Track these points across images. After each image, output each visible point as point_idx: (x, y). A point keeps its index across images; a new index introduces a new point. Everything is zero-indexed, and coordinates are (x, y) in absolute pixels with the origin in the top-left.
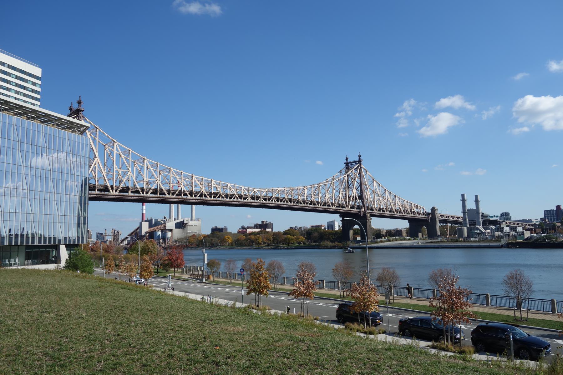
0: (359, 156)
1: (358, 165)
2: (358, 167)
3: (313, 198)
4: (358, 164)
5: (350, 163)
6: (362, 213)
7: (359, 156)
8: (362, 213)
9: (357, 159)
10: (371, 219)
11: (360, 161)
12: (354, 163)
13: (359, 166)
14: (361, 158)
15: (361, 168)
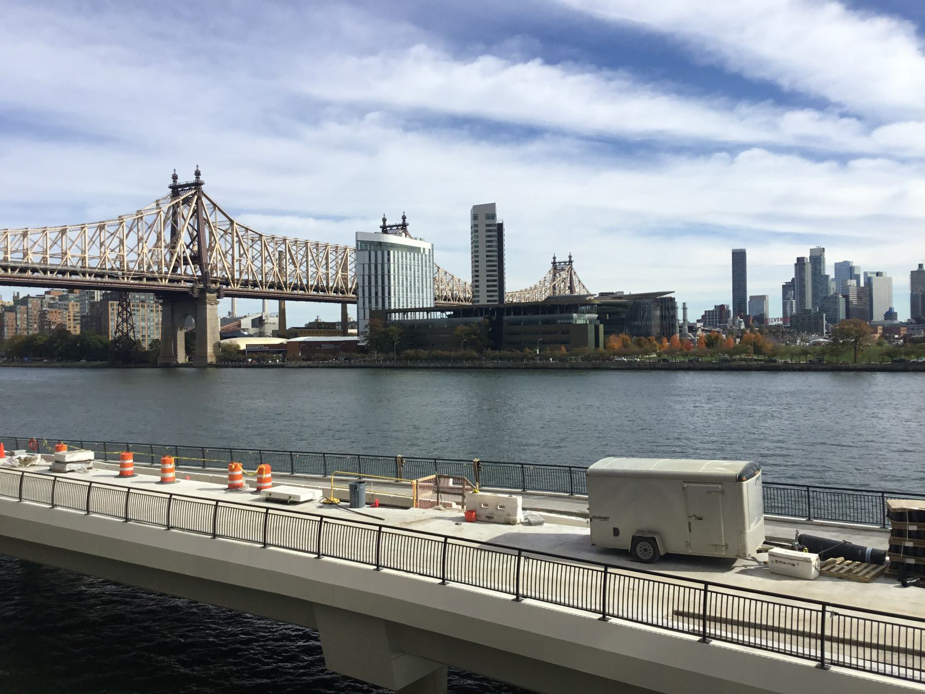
0: (198, 174)
1: (193, 192)
2: (193, 195)
3: (30, 256)
4: (195, 189)
5: (182, 186)
6: (196, 291)
7: (198, 174)
8: (196, 291)
9: (192, 179)
10: (217, 303)
11: (197, 185)
12: (188, 188)
13: (195, 193)
14: (202, 178)
15: (199, 198)
